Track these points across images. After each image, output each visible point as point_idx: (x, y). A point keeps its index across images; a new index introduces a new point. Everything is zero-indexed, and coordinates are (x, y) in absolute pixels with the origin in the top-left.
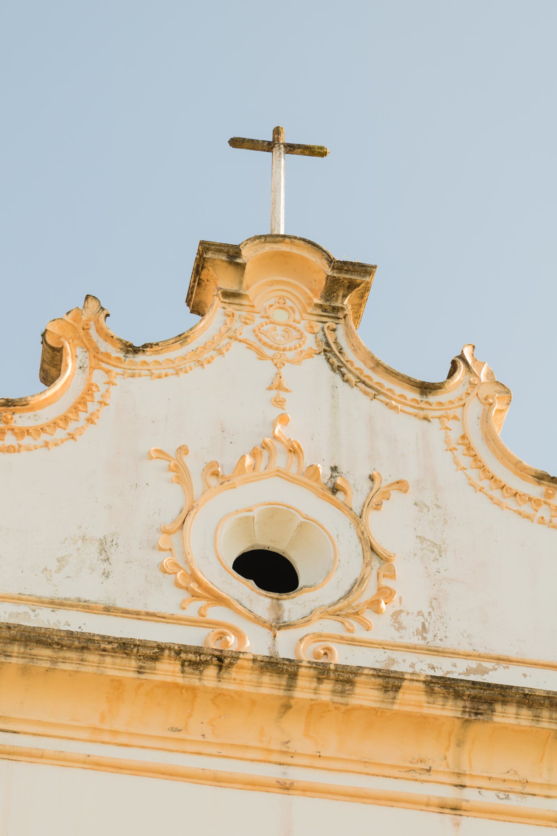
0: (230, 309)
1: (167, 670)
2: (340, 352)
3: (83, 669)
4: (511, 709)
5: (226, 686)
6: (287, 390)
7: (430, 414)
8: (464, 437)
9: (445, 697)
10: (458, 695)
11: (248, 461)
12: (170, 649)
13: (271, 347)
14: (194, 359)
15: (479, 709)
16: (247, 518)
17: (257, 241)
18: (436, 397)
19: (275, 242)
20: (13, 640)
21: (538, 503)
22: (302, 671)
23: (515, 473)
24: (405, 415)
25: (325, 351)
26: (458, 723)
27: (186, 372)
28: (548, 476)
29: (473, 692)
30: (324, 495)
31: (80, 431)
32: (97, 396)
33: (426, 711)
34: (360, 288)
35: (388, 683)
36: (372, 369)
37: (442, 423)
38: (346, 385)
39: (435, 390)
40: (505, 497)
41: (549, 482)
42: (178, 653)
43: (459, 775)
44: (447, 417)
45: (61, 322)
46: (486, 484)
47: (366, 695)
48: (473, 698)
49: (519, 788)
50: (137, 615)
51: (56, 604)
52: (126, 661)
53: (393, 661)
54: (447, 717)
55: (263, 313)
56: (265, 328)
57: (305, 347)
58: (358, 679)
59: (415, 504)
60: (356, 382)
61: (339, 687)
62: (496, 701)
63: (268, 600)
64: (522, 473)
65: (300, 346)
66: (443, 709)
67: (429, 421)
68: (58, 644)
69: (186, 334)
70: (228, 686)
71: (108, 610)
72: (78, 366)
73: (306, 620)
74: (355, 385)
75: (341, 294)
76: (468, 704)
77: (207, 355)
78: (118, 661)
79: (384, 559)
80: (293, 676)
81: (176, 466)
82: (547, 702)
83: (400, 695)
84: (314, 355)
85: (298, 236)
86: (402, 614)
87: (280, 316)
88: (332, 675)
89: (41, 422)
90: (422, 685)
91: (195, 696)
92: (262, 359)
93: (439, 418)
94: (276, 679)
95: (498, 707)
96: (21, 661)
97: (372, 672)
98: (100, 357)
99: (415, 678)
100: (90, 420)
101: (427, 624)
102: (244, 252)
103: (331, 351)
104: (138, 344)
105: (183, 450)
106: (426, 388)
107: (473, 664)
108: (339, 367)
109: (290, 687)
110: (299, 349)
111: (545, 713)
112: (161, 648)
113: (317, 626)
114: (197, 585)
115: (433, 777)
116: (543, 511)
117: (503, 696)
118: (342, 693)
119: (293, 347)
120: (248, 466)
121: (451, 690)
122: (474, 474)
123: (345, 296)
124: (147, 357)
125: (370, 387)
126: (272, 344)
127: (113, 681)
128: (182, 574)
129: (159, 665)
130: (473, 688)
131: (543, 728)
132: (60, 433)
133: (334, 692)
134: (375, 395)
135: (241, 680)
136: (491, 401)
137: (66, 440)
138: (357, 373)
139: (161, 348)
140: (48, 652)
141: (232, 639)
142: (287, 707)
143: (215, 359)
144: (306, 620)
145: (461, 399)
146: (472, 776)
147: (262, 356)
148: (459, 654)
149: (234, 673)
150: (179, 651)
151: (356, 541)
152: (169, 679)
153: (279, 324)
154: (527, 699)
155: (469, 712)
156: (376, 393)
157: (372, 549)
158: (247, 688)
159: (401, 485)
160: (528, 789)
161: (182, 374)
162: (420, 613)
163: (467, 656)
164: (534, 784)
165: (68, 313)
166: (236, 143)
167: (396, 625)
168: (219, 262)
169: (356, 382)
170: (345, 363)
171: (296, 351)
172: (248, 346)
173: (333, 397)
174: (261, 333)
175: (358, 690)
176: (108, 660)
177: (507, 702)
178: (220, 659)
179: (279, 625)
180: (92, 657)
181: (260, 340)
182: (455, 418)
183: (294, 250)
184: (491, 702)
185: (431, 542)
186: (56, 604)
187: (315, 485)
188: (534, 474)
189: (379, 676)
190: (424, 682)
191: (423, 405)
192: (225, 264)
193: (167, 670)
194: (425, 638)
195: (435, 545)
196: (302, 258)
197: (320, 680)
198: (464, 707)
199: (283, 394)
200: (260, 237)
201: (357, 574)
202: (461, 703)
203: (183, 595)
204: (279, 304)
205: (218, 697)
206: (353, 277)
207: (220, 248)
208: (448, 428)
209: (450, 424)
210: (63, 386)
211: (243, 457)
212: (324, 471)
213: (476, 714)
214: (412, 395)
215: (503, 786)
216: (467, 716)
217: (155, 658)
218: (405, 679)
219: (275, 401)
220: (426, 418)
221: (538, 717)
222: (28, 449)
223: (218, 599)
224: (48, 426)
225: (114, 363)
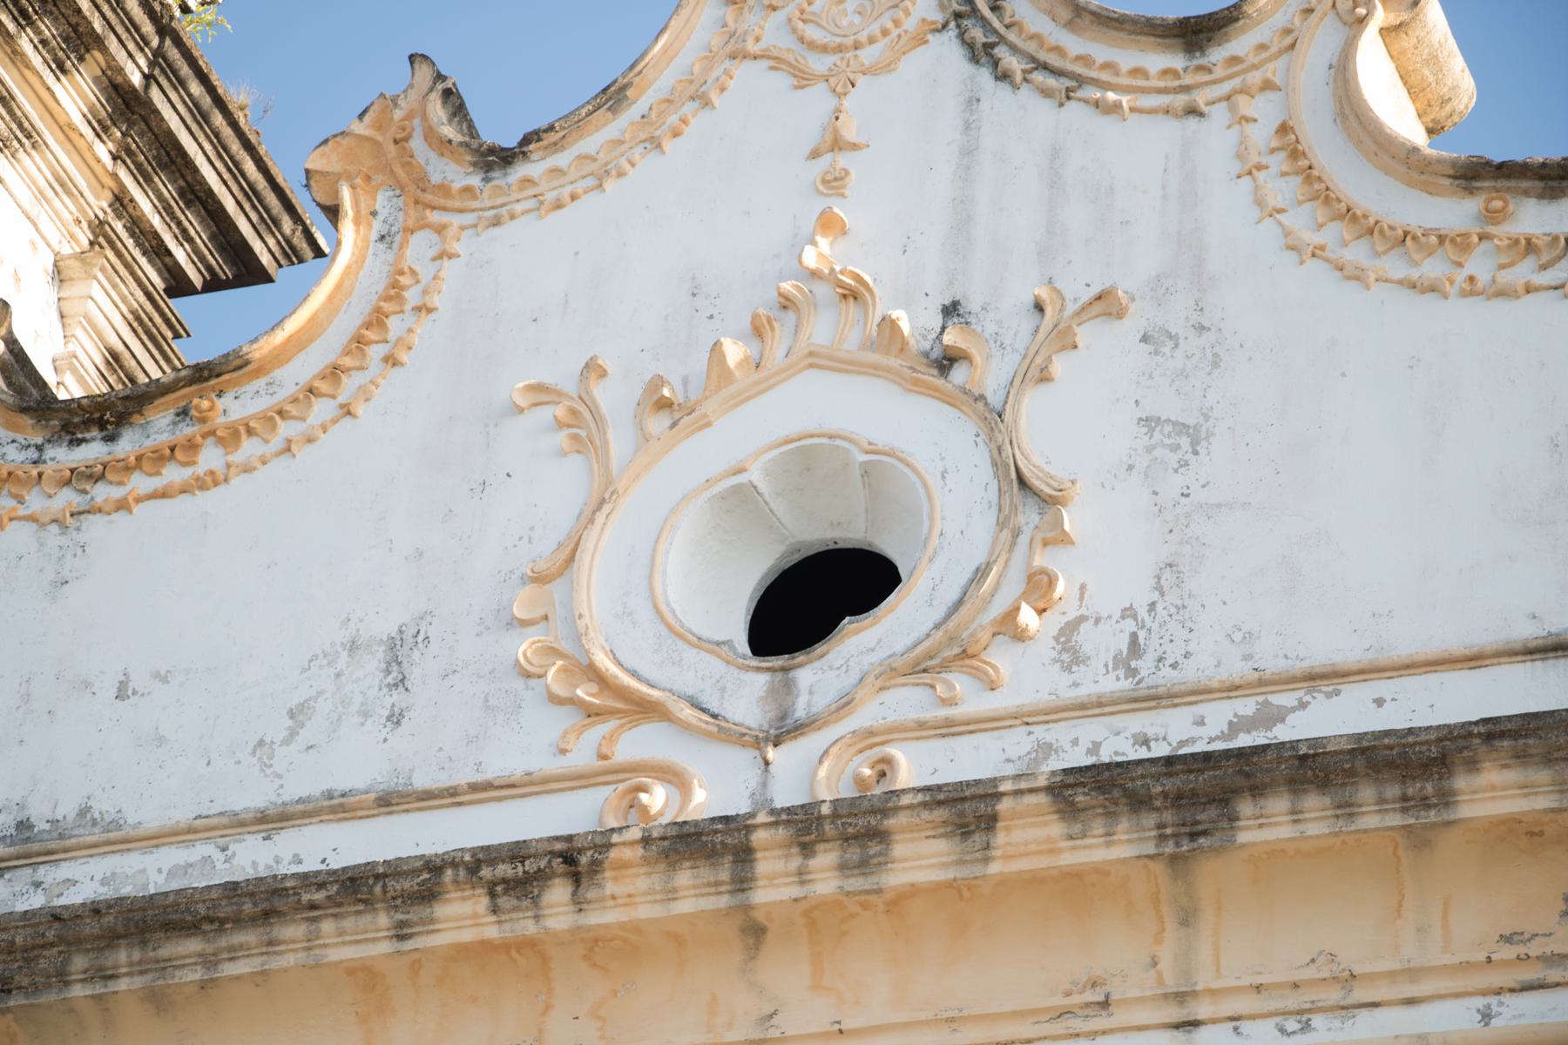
1: (462, 917)
3: (276, 963)
4: (1278, 804)
5: (597, 918)
6: (855, 147)
7: (1200, 98)
8: (1284, 129)
9: (1110, 815)
10: (1139, 802)
11: (734, 352)
12: (454, 864)
13: (824, 49)
14: (643, 136)
15: (1197, 823)
16: (737, 489)
18: (1227, 45)
20: (112, 938)
21: (1460, 243)
22: (759, 837)
23: (1410, 183)
24: (1144, 116)
25: (958, 16)
26: (1159, 868)
27: (621, 174)
29: (1170, 784)
30: (916, 382)
31: (365, 394)
32: (412, 296)
33: (1073, 857)
35: (962, 815)
36: (1070, 25)
37: (1233, 109)
38: (1004, 89)
39: (1220, 28)
40: (1377, 254)
42: (474, 869)
43: (1180, 997)
45: (345, 141)
46: (1331, 234)
47: (919, 857)
48: (1177, 799)
49: (1334, 996)
50: (450, 796)
51: (270, 820)
52: (365, 920)
53: (1047, 749)
54: (1123, 861)
57: (910, 24)
58: (891, 823)
59: (1145, 339)
60: (1024, 71)
61: (854, 853)
62: (1236, 791)
63: (763, 678)
64: (1424, 177)
65: (897, 23)
66: (1109, 844)
67: (1201, 115)
68: (211, 920)
69: (622, 81)
70: (601, 917)
71: (388, 802)
72: (374, 236)
73: (845, 704)
74: (1025, 80)
76: (1168, 816)
77: (673, 119)
78: (348, 923)
79: (1049, 502)
80: (744, 855)
81: (573, 412)
82: (1360, 763)
83: (1000, 838)
84: (930, 37)
86: (1084, 627)
88: (828, 828)
89: (283, 394)
90: (1042, 799)
91: (545, 960)
92: (802, 87)
93: (1228, 98)
94: (706, 873)
95: (1245, 807)
96: (138, 982)
97: (920, 797)
98: (428, 197)
99: (1023, 785)
100: (391, 361)
101: (1142, 635)
103: (975, 11)
104: (510, 141)
105: (593, 369)
107: (1247, 706)
108: (988, 47)
109: (742, 882)
110: (895, 32)
111: (1366, 793)
112: (434, 866)
113: (868, 714)
114: (594, 688)
115: (1119, 1018)
116: (1480, 265)
117: (1248, 775)
118: (864, 866)
119: (878, 33)
120: (740, 364)
121: (1116, 793)
122: (1301, 220)
124: (532, 168)
126: (838, 40)
127: (351, 972)
128: (563, 670)
129: (442, 910)
130: (1169, 775)
131: (1365, 831)
132: (322, 409)
133: (843, 868)
134: (1068, 90)
135: (630, 896)
136: (1362, 11)
137: (335, 421)
138: (1031, 47)
139: (561, 134)
140: (193, 945)
141: (657, 798)
142: (755, 933)
143: (692, 121)
144: (845, 704)
146: (1212, 993)
147: (803, 79)
148: (1210, 691)
149: (611, 885)
150: (475, 865)
151: (985, 472)
152: (467, 936)
154: (1311, 769)
155: (1174, 835)
156: (1068, 83)
157: (1022, 481)
158: (645, 912)
159: (1105, 304)
160: (1360, 994)
161: (610, 185)
162: (1129, 612)
163: (1232, 690)
164: (1371, 977)
165: (361, 116)
167: (1066, 657)
169: (1024, 71)
170: (1002, 30)
171: (888, 39)
172: (772, 63)
173: (967, 126)
174: (804, 21)
175: (899, 849)
176: (327, 926)
177: (1265, 786)
178: (569, 859)
179: (784, 730)
180: (292, 931)
181: (802, 40)
184: (1224, 799)
185: (1175, 423)
186: (270, 820)
187: (894, 362)
189: (940, 803)
190: (1049, 789)
191: (1188, 80)
193: (462, 917)
194: (1132, 672)
195: (1181, 428)
197: (807, 849)
198: (1160, 826)
199: (843, 160)
201: (980, 558)
202: (1150, 820)
203: (565, 718)
205: (595, 948)
208: (1247, 119)
209: (1245, 105)
210: (330, 298)
211: (716, 347)
212: (915, 322)
213: (1194, 836)
214: (1160, 60)
215: (1293, 1001)
216: (1169, 848)
217: (428, 895)
218: (1003, 794)
219: (824, 182)
220: (1193, 111)
221: (1350, 805)
222: (247, 469)
223: (644, 709)
224: (295, 401)
225: (458, 204)
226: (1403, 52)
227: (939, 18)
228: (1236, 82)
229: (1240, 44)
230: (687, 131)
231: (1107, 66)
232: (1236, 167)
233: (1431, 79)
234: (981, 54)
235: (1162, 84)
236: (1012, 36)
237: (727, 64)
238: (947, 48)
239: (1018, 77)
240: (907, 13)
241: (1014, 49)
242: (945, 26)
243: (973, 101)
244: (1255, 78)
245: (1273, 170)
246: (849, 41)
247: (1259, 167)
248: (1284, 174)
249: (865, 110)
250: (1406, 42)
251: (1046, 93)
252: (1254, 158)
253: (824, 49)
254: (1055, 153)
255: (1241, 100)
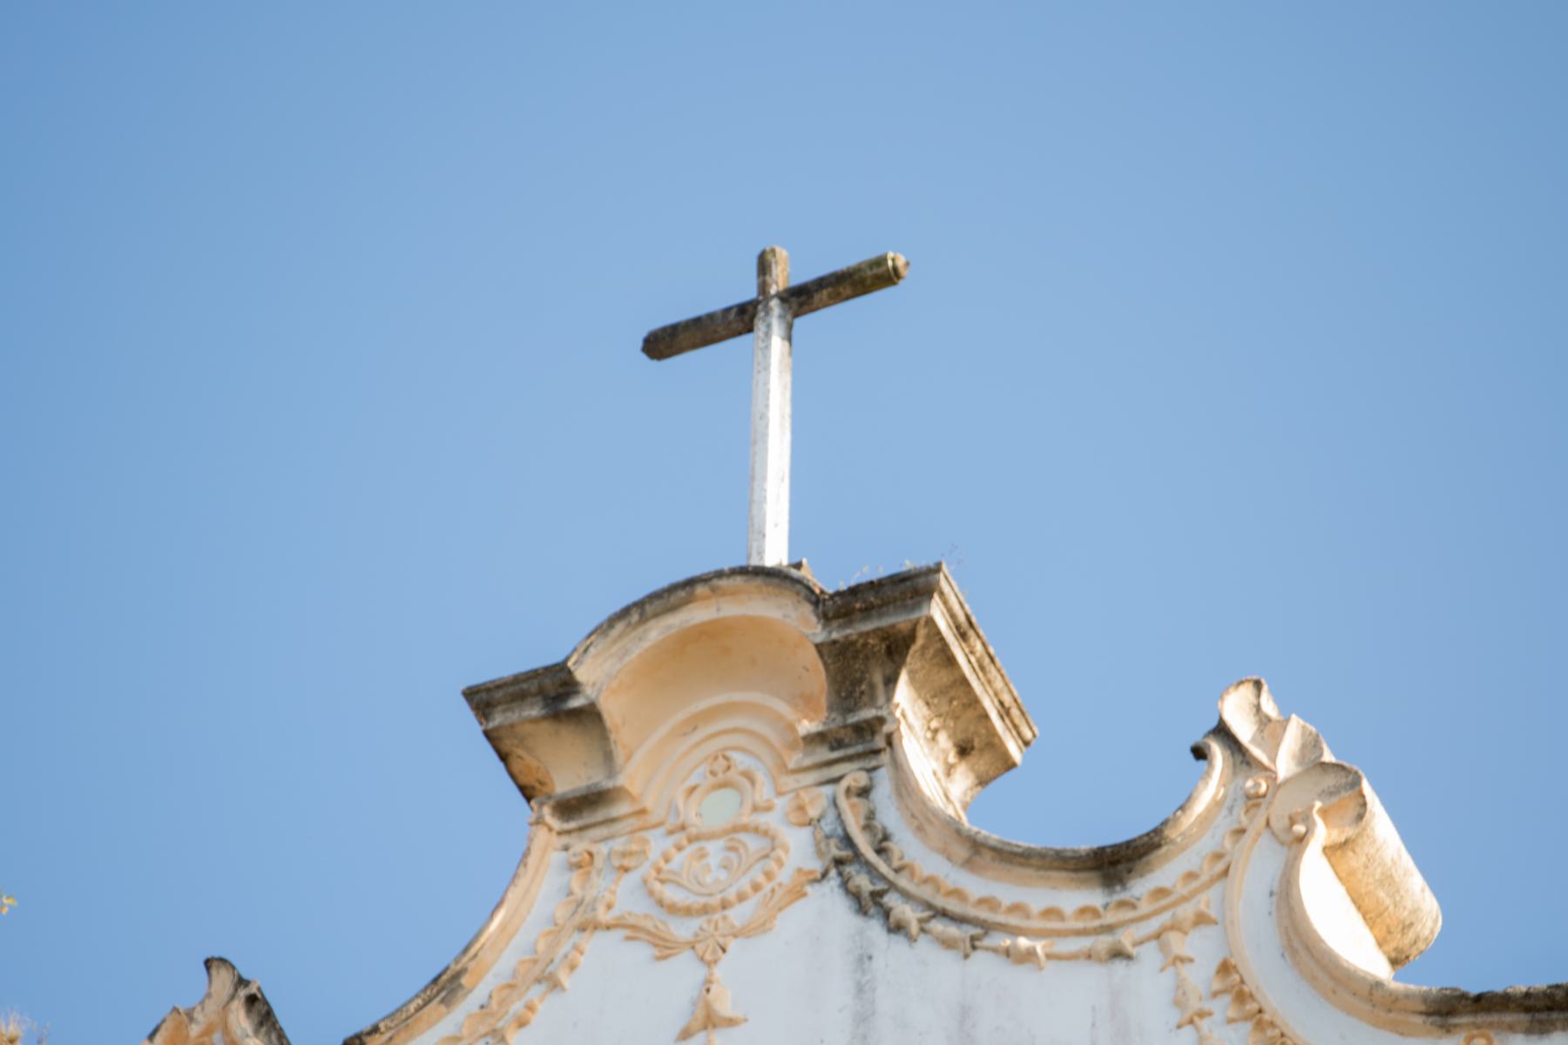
0: (580, 845)
2: (880, 851)
6: (731, 1022)
7: (1126, 938)
8: (1225, 968)
13: (688, 912)
14: (483, 1029)
17: (620, 627)
18: (1150, 876)
19: (673, 609)
23: (1377, 1024)
24: (1063, 964)
25: (839, 862)
28: (1463, 996)
34: (920, 641)
36: (968, 864)
37: (1164, 948)
38: (898, 942)
39: (1141, 856)
41: (1475, 1012)
44: (1174, 927)
55: (672, 822)
56: (678, 859)
57: (785, 876)
60: (921, 921)
64: (1392, 1015)
65: (769, 875)
67: (1129, 957)
69: (455, 968)
74: (923, 930)
75: (878, 678)
77: (517, 1007)
84: (809, 889)
85: (726, 567)
87: (718, 809)
92: (665, 958)
93: (1158, 936)
102: (581, 674)
103: (857, 856)
106: (1114, 864)
108: (876, 896)
110: (768, 887)
119: (748, 889)
123: (891, 681)
125: (960, 920)
126: (703, 900)
134: (973, 939)
136: (1300, 828)
138: (926, 892)
139: (388, 1035)
143: (540, 1007)
145: (1218, 856)
147: (664, 948)
153: (711, 836)
166: (661, 344)
168: (529, 728)
169: (921, 921)
170: (891, 875)
171: (759, 895)
172: (628, 932)
173: (860, 990)
174: (662, 882)
181: (660, 903)
182: (1201, 920)
183: (729, 609)
188: (1422, 1008)
191: (1110, 918)
192: (546, 726)
196: (757, 623)
200: (625, 613)
204: (715, 777)
206: (885, 622)
207: (515, 690)
208: (1182, 960)
209: (1179, 944)
214: (1076, 897)
220: (1118, 954)
226: (1352, 873)
227: (817, 866)
228: (1166, 917)
229: (1164, 873)
230: (535, 1020)
231: (1016, 908)
232: (1174, 1016)
233: (1388, 901)
234: (870, 904)
235: (1080, 925)
236: (903, 881)
237: (576, 937)
238: (829, 901)
239: (914, 928)
240: (780, 863)
241: (907, 896)
242: (825, 875)
243: (864, 959)
244: (1187, 911)
245: (1218, 1016)
246: (715, 901)
247: (1202, 1014)
248: (1231, 1021)
249: (741, 977)
250: (1354, 861)
251: (948, 944)
252: (1194, 1005)
253: (688, 912)
254: (965, 1013)
255: (1173, 937)
